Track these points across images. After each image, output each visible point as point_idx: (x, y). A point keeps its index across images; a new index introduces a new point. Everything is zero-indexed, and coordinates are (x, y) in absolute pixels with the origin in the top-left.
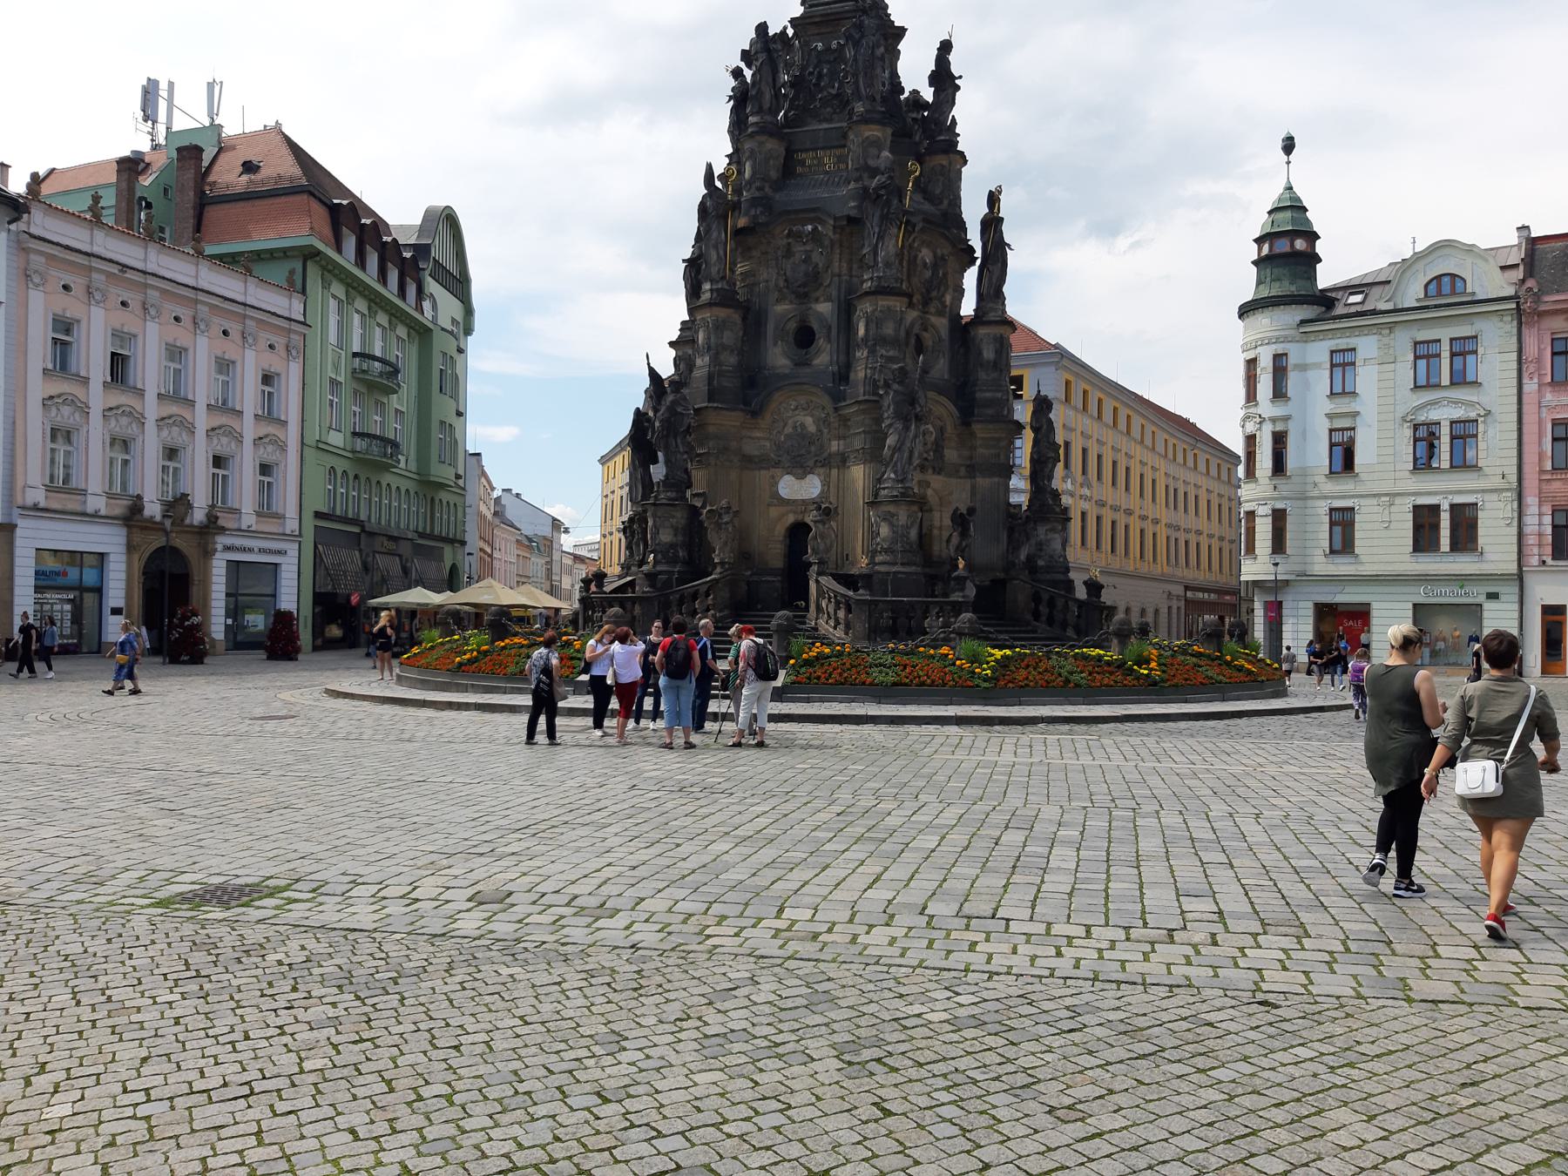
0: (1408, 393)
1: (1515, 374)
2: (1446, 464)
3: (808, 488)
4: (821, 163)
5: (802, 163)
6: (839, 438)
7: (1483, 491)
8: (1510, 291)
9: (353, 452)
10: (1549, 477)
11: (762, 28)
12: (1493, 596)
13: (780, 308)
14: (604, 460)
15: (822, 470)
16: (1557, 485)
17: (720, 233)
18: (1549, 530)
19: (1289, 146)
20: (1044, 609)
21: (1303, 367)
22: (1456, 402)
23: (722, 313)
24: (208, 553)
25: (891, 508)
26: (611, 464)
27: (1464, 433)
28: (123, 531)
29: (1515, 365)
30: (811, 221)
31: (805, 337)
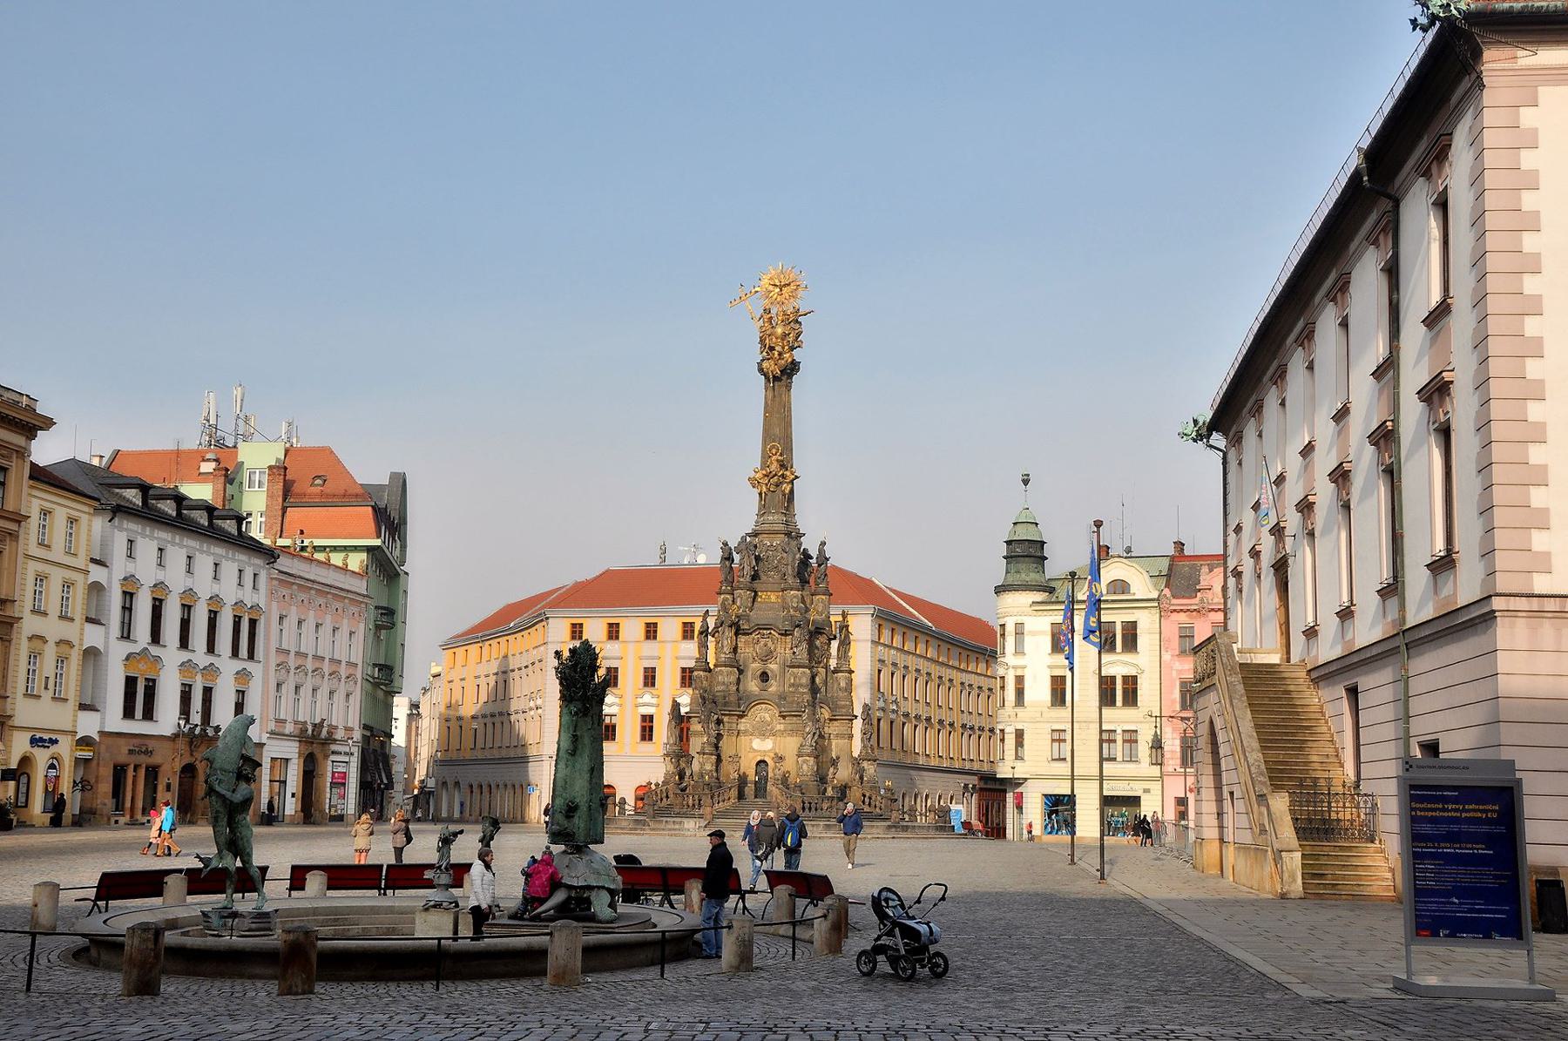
5: (761, 597)
8: (1155, 595)
9: (374, 678)
11: (743, 539)
12: (1147, 791)
14: (446, 646)
18: (1178, 749)
19: (1026, 482)
20: (867, 800)
21: (1034, 633)
22: (1126, 663)
24: (326, 757)
25: (808, 758)
26: (460, 651)
28: (297, 744)
30: (769, 629)
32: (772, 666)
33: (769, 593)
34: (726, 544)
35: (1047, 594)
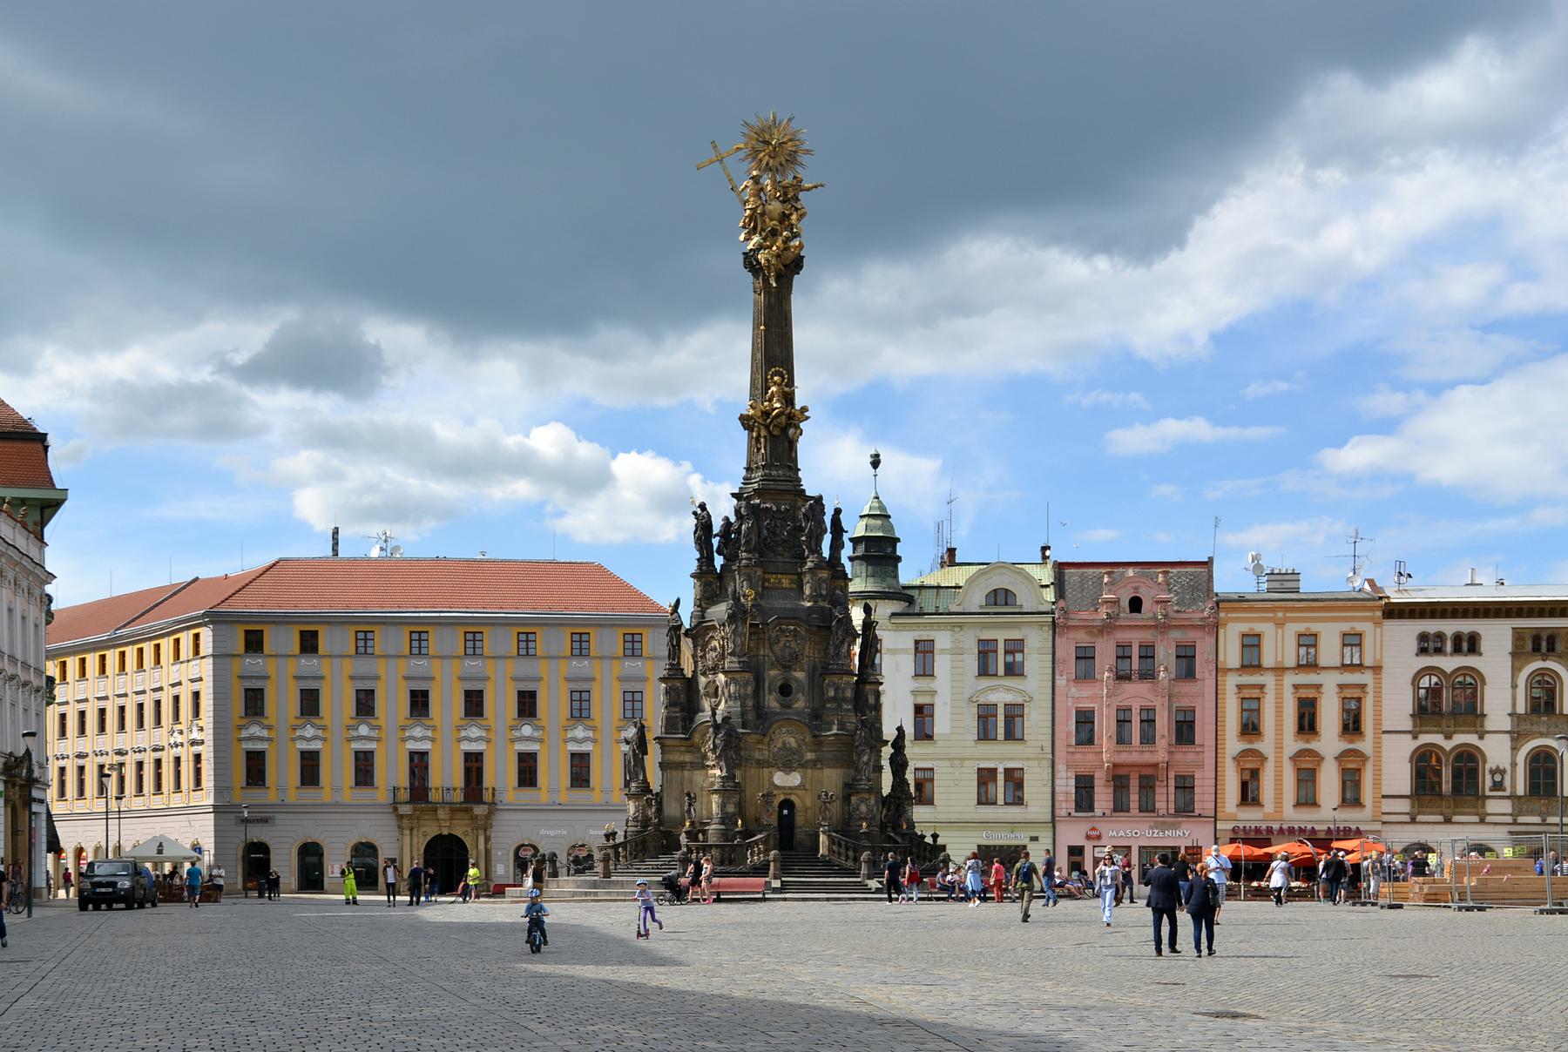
0: (973, 679)
1: (1050, 671)
2: (1001, 736)
3: (794, 779)
4: (780, 582)
6: (811, 751)
7: (1028, 759)
10: (1074, 750)
13: (773, 673)
15: (801, 770)
16: (1078, 756)
17: (743, 629)
18: (1073, 791)
19: (876, 463)
21: (894, 652)
22: (1009, 689)
23: (747, 675)
25: (867, 796)
27: (1014, 714)
29: (1050, 664)
31: (785, 690)
32: (800, 675)
33: (779, 576)
34: (703, 507)
35: (907, 604)
